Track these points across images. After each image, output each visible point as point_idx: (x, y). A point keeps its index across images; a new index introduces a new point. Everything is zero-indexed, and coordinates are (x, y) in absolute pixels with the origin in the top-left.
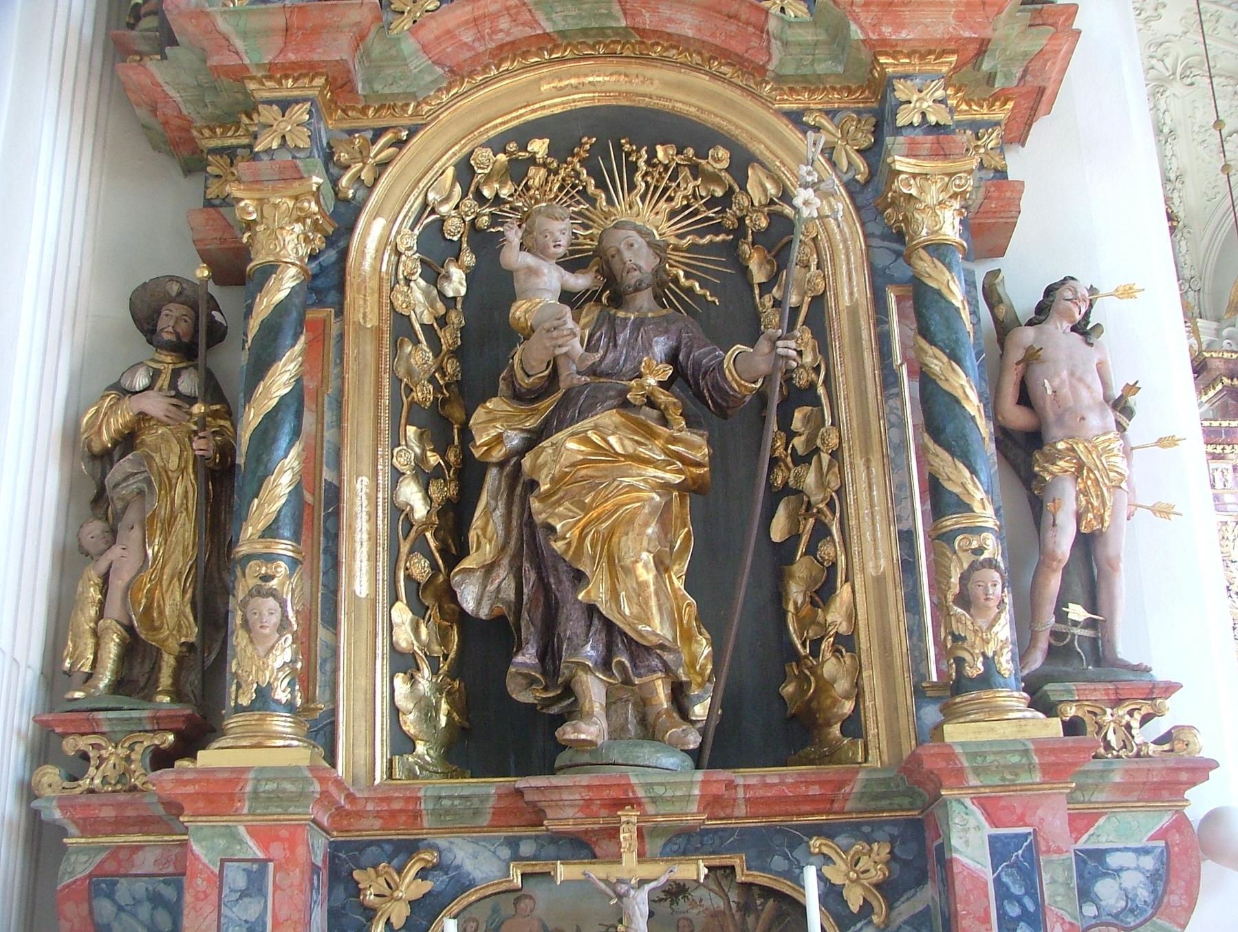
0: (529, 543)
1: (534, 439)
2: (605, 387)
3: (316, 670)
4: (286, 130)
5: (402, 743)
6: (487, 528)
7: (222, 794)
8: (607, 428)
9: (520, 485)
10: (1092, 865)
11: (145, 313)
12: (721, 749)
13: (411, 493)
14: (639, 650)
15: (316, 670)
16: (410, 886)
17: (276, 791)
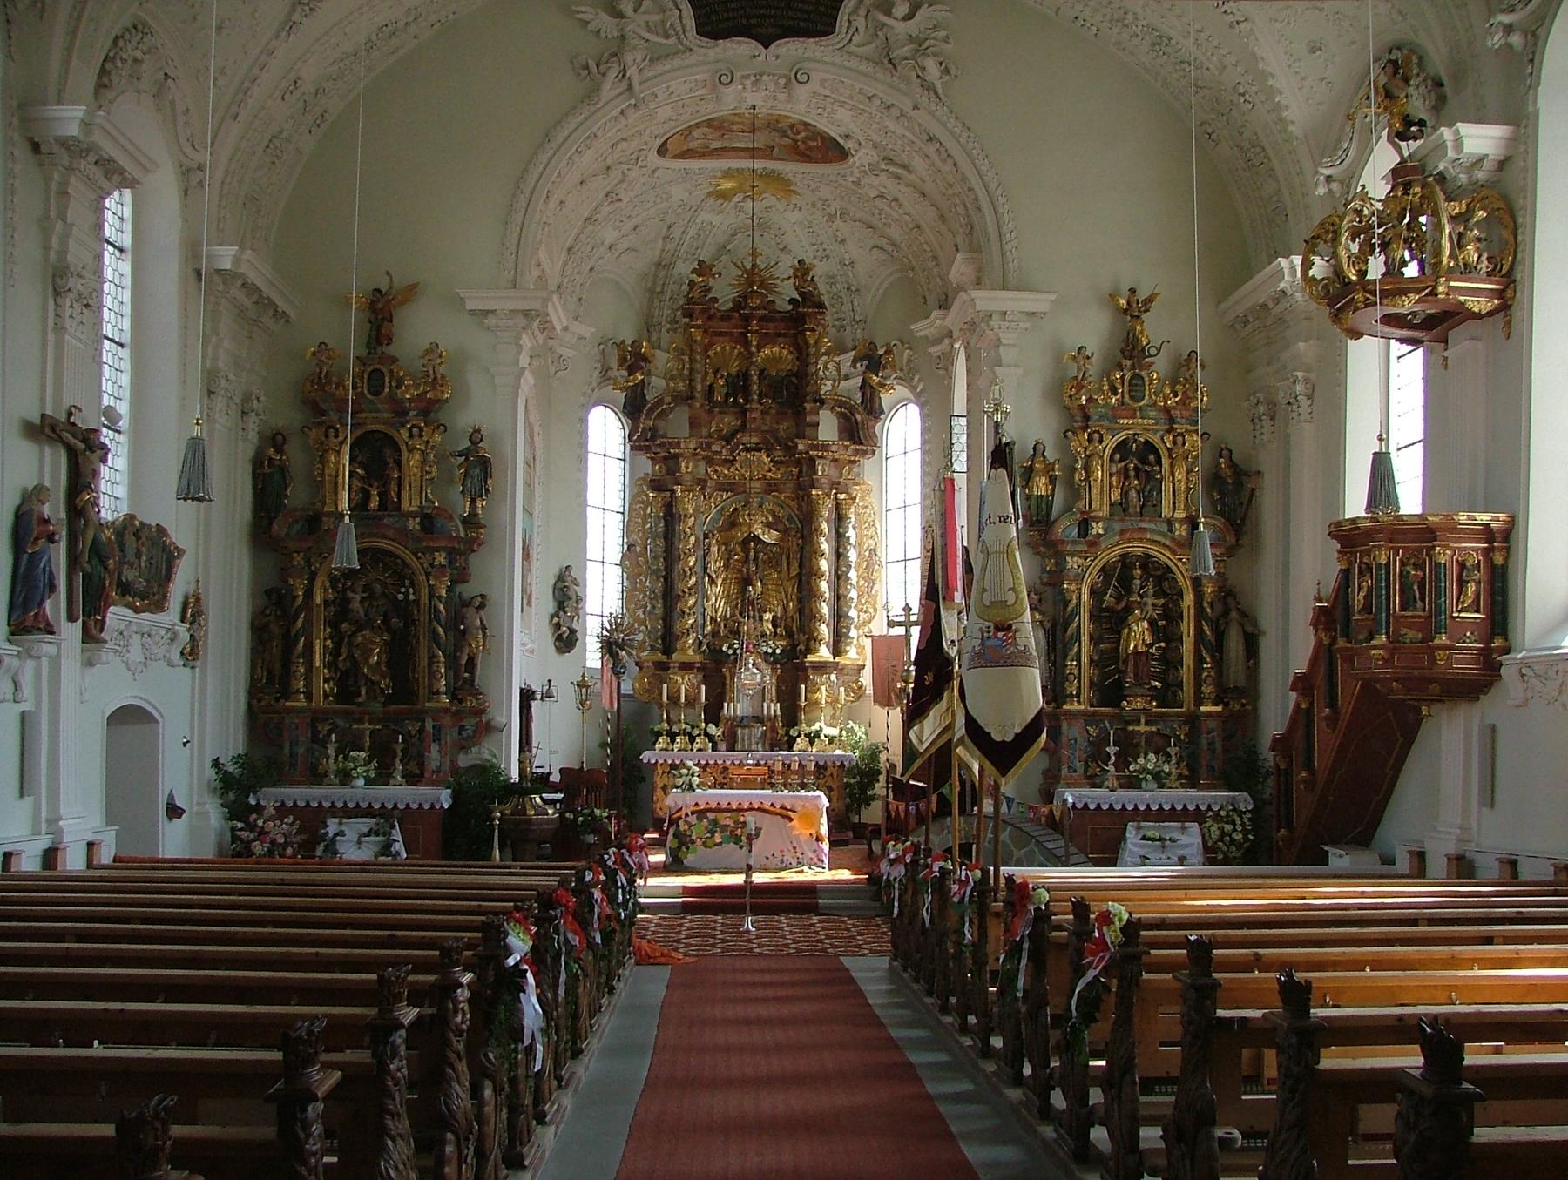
0: (351, 656)
1: (354, 633)
2: (367, 623)
3: (308, 684)
4: (298, 559)
5: (326, 696)
6: (344, 650)
7: (291, 710)
8: (367, 633)
9: (350, 644)
10: (462, 728)
11: (268, 593)
12: (390, 700)
13: (329, 643)
14: (372, 682)
15: (308, 684)
16: (327, 727)
17: (299, 711)
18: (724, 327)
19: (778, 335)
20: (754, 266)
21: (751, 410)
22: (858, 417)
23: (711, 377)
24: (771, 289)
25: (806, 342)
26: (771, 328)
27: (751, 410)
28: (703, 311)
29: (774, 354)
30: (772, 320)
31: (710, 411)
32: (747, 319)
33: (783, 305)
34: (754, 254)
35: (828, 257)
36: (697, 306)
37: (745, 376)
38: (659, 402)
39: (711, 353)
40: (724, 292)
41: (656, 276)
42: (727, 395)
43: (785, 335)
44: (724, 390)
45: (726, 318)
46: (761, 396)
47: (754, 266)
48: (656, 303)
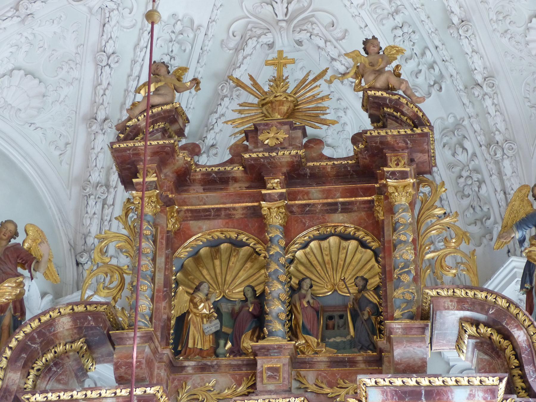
18: (212, 200)
19: (332, 208)
20: (279, 81)
21: (267, 351)
22: (520, 336)
23: (181, 301)
24: (317, 117)
25: (391, 210)
26: (315, 196)
27: (267, 351)
28: (164, 156)
29: (334, 262)
30: (317, 177)
31: (175, 368)
32: (257, 175)
33: (339, 146)
34: (280, 62)
35: (438, 83)
36: (149, 145)
37: (261, 299)
38: (46, 336)
39: (183, 253)
40: (216, 141)
41: (89, 149)
42: (218, 335)
43: (346, 208)
44: (213, 326)
45: (216, 180)
46: (293, 333)
47: (279, 81)
48: (94, 207)
